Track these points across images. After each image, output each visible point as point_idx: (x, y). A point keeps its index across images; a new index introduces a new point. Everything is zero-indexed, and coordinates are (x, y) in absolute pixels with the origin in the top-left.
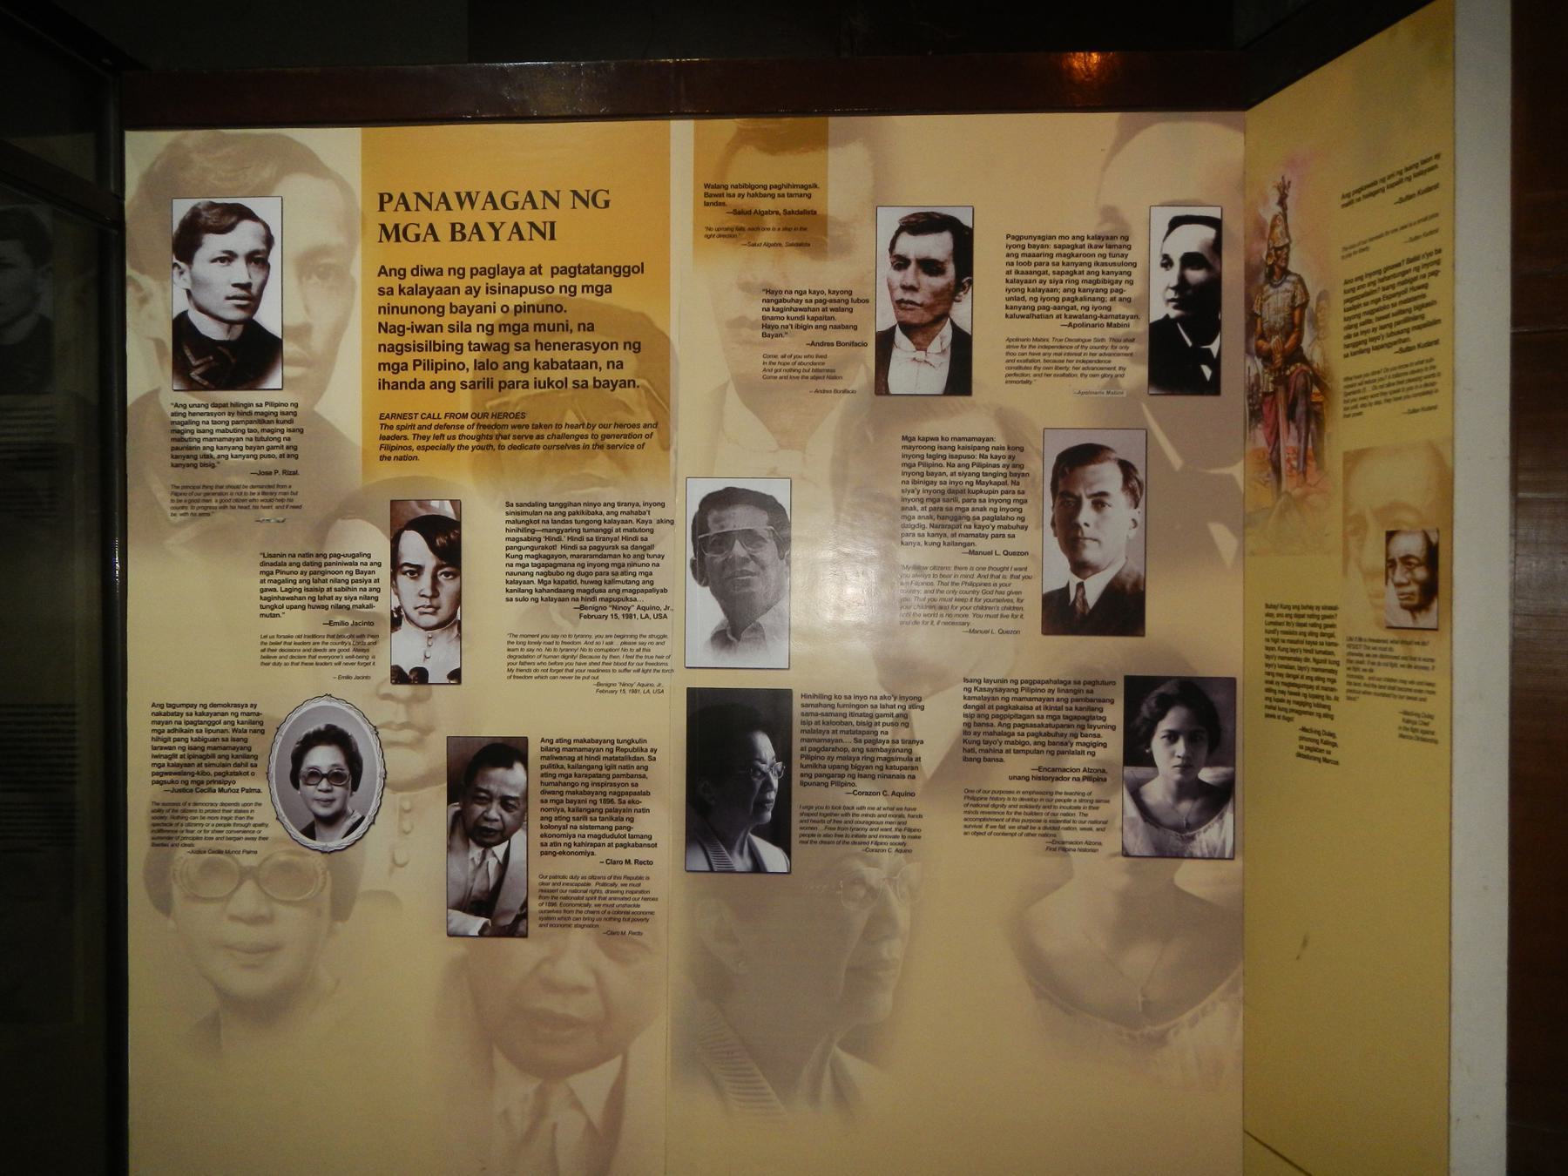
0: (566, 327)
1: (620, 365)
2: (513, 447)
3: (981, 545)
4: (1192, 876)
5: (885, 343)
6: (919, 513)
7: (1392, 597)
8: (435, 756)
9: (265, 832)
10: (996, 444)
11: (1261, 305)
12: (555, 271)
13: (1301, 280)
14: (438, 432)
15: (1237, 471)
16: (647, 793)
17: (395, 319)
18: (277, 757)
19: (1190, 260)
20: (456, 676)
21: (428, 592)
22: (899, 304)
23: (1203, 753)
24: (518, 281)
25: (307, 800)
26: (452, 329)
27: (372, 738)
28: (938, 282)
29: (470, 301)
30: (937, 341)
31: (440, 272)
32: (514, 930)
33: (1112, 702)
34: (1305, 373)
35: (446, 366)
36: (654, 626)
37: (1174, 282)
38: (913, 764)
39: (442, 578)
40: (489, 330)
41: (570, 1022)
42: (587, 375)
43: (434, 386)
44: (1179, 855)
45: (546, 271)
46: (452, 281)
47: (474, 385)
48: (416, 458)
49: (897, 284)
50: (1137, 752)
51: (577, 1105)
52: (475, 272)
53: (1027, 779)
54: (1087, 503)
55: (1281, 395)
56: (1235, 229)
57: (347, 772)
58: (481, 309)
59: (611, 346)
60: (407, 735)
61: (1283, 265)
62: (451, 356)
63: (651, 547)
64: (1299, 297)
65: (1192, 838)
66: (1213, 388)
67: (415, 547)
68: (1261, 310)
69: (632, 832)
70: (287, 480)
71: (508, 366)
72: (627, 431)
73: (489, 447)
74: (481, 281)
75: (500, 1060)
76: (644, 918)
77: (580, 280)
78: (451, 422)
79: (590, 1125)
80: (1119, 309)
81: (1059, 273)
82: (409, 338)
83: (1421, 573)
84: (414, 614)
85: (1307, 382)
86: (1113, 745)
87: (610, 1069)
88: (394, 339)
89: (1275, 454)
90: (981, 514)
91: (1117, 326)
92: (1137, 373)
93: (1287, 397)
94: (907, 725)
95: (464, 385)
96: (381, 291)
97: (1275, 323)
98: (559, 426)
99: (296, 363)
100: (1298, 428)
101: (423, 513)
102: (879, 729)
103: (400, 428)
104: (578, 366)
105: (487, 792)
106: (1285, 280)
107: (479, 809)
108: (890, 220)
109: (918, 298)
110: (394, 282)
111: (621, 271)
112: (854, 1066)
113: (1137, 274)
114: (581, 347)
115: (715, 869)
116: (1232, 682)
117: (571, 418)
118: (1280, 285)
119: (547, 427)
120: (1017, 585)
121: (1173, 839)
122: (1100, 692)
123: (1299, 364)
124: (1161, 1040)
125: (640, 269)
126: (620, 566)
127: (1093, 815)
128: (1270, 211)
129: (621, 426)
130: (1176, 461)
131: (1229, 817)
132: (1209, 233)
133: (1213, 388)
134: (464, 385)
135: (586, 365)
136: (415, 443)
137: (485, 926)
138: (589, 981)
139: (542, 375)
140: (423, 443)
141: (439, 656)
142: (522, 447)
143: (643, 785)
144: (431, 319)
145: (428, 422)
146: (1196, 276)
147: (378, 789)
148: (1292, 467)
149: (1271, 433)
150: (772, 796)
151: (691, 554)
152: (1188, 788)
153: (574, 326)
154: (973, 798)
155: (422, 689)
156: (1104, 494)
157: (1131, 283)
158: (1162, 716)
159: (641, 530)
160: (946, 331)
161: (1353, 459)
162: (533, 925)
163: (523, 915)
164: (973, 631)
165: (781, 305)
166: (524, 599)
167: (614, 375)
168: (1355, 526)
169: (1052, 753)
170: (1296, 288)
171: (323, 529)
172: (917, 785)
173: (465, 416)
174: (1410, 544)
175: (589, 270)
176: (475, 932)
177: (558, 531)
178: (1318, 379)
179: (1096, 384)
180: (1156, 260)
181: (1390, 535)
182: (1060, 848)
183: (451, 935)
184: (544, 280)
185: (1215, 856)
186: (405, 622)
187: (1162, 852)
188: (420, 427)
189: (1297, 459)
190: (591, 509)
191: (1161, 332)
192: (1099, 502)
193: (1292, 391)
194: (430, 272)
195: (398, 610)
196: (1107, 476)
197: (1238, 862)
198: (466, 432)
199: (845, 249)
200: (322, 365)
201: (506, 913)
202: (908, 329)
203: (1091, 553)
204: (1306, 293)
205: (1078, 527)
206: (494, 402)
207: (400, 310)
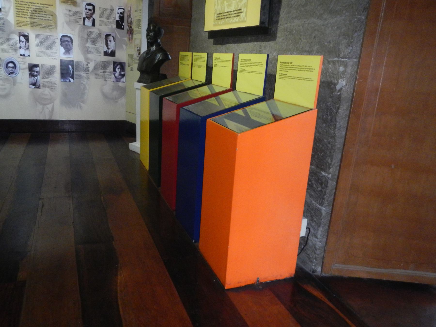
0: (42, 12)
1: (50, 18)
2: (36, 27)
3: (96, 45)
4: (120, 84)
5: (84, 19)
6: (89, 40)
7: (137, 54)
8: (27, 66)
9: (3, 74)
10: (98, 33)
12: (41, 4)
13: (131, 18)
14: (25, 24)
15: (126, 39)
16: (55, 72)
17: (18, 8)
18: (4, 64)
19: (121, 13)
20: (29, 56)
21: (25, 45)
22: (86, 14)
23: (122, 71)
24: (35, 5)
25: (8, 70)
26: (26, 10)
27: (18, 63)
28: (91, 12)
29: (28, 6)
30: (91, 19)
31: (24, 2)
32: (38, 88)
33: (112, 64)
35: (26, 15)
36: (56, 51)
37: (119, 16)
38: (88, 70)
39: (26, 43)
40: (32, 11)
41: (47, 99)
42: (46, 18)
43: (24, 17)
44: (119, 82)
45: (39, 4)
46: (26, 4)
47: (30, 18)
48: (22, 27)
49: (86, 11)
50: (114, 70)
51: (48, 109)
52: (29, 3)
53: (102, 72)
54: (109, 41)
55: (130, 31)
56: (126, 10)
57: (14, 67)
58: (30, 8)
59: (48, 15)
60: (23, 63)
62: (26, 14)
63: (55, 41)
65: (120, 80)
66: (123, 29)
67: (22, 38)
69: (54, 76)
70: (3, 28)
71: (34, 16)
72: (51, 26)
73: (32, 26)
74: (30, 4)
75: (37, 103)
76: (55, 87)
77: (44, 6)
78: (26, 22)
79: (50, 111)
80: (113, 18)
81: (105, 13)
82: (20, 10)
83: (139, 51)
84: (23, 47)
86: (112, 69)
87: (52, 104)
88: (18, 10)
90: (96, 41)
91: (112, 20)
92: (115, 26)
94: (88, 65)
95: (28, 18)
96: (16, 4)
98: (42, 25)
99: (4, 12)
101: (23, 34)
102: (84, 66)
103: (19, 22)
104: (44, 17)
105: (34, 71)
107: (33, 73)
108: (85, 4)
109: (88, 14)
110: (17, 2)
111: (49, 5)
112: (81, 104)
113: (115, 14)
114: (45, 14)
115: (64, 81)
116: (125, 63)
117: (43, 24)
119: (40, 25)
120: (100, 50)
121: (118, 80)
122: (110, 63)
124: (117, 102)
125: (52, 5)
126: (51, 43)
127: (109, 77)
128: (129, 9)
129: (50, 25)
130: (119, 37)
131: (125, 78)
132: (123, 10)
133: (123, 29)
134: (28, 18)
135: (45, 17)
136: (21, 25)
137: (35, 87)
138: (49, 94)
139: (39, 18)
140: (22, 25)
141: (26, 53)
142: (37, 27)
143: (55, 71)
144: (23, 8)
145: (23, 22)
146: (121, 15)
147: (19, 69)
150: (71, 73)
151: (60, 43)
152: (120, 74)
153: (43, 12)
154: (96, 74)
155: (24, 57)
156: (111, 40)
157: (114, 15)
158: (117, 66)
159: (54, 39)
160: (92, 18)
161: (135, 39)
162: (41, 87)
163: (40, 86)
164: (96, 55)
165: (71, 12)
166: (38, 47)
167: (49, 19)
168: (135, 46)
169: (105, 70)
171: (9, 35)
172: (89, 73)
173: (28, 22)
174: (139, 48)
175: (45, 5)
176: (33, 88)
177: (42, 38)
178: (133, 30)
179: (110, 27)
180: (117, 13)
181: (137, 47)
182: (106, 81)
183: (30, 88)
184: (39, 5)
185: (123, 82)
186: (21, 48)
187: (117, 81)
188: (23, 23)
190: (47, 36)
191: (117, 21)
192: (110, 41)
194: (23, 2)
195: (20, 47)
196: (111, 38)
197: (125, 83)
198: (29, 24)
199: (79, 6)
200: (7, 13)
201: (37, 85)
202: (87, 17)
203: (109, 47)
204: (132, 20)
205: (108, 44)
206: (33, 20)
207: (19, 6)
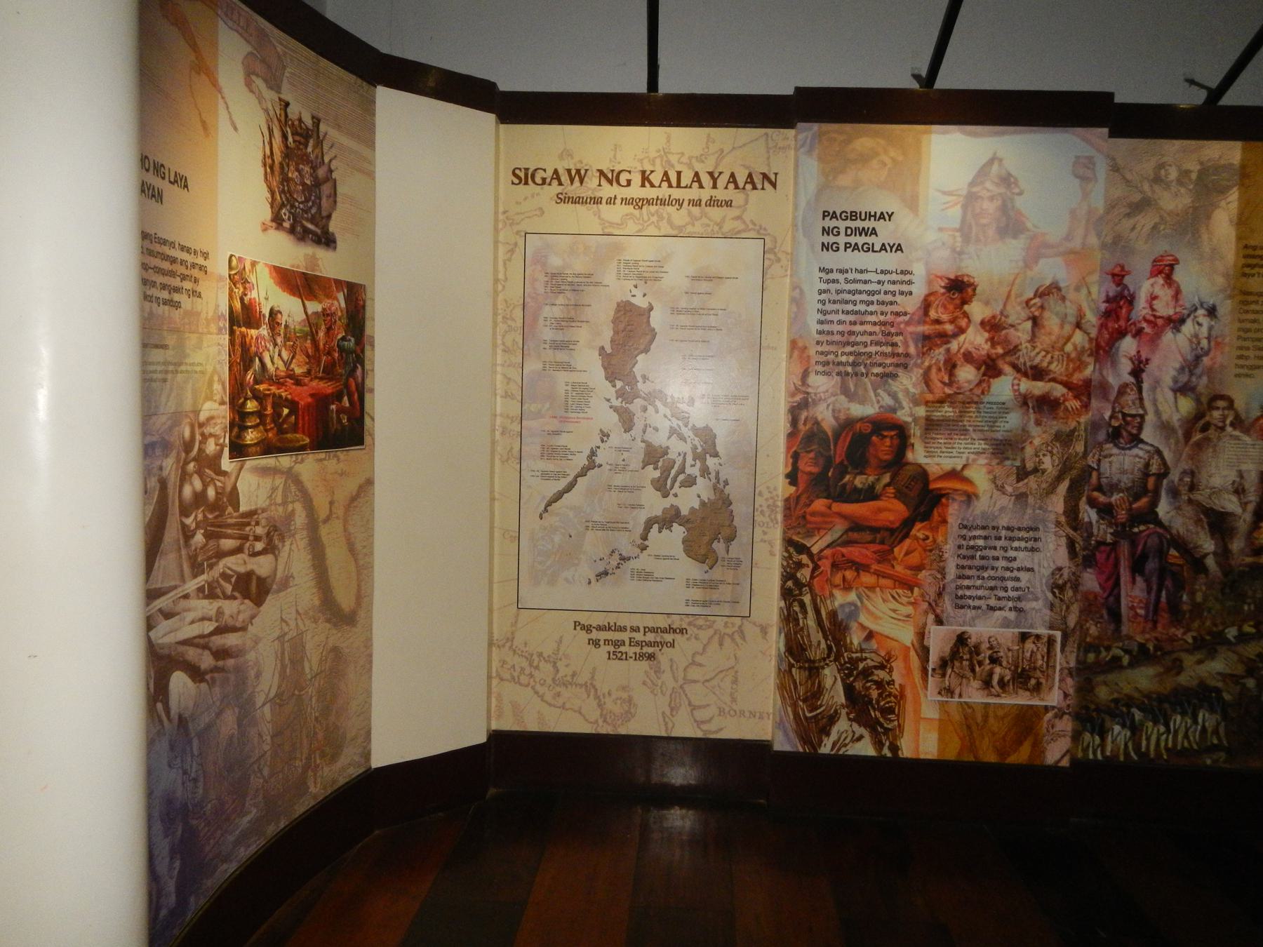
11: (1099, 461)
34: (1160, 536)
55: (1125, 548)
61: (1134, 431)
64: (1155, 466)
68: (1099, 465)
85: (1161, 542)
89: (1111, 599)
93: (1132, 554)
97: (1120, 481)
100: (1148, 582)
106: (1136, 446)
118: (1130, 449)
123: (1152, 526)
148: (1137, 615)
149: (1108, 579)
170: (1151, 458)
189: (1146, 608)
193: (1140, 547)
